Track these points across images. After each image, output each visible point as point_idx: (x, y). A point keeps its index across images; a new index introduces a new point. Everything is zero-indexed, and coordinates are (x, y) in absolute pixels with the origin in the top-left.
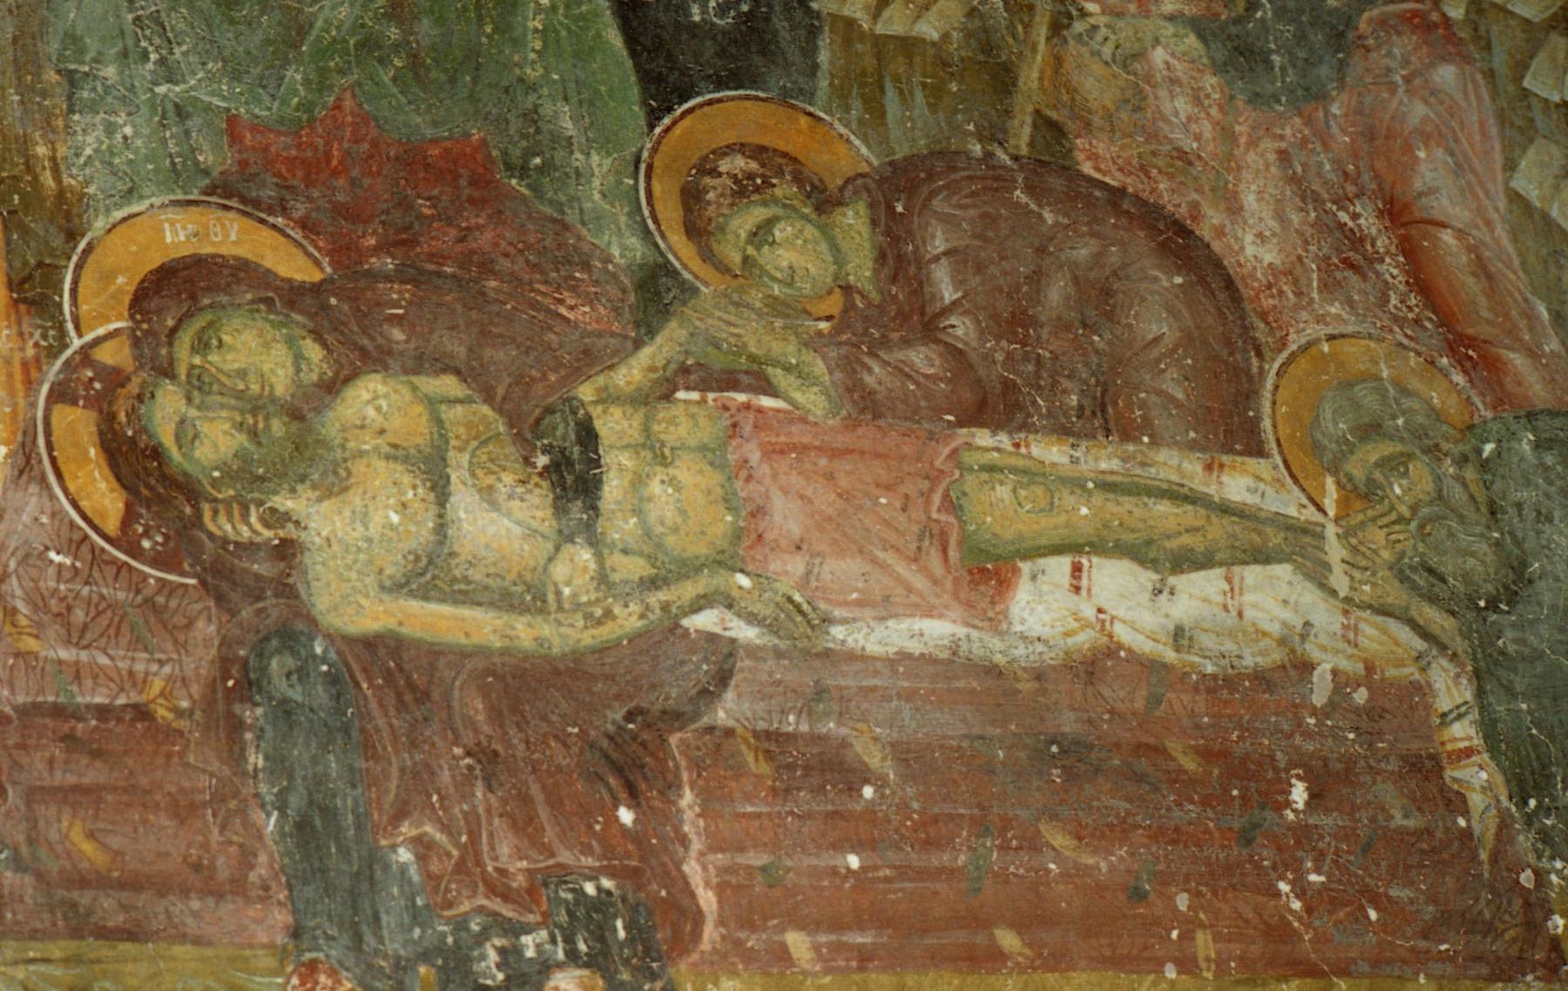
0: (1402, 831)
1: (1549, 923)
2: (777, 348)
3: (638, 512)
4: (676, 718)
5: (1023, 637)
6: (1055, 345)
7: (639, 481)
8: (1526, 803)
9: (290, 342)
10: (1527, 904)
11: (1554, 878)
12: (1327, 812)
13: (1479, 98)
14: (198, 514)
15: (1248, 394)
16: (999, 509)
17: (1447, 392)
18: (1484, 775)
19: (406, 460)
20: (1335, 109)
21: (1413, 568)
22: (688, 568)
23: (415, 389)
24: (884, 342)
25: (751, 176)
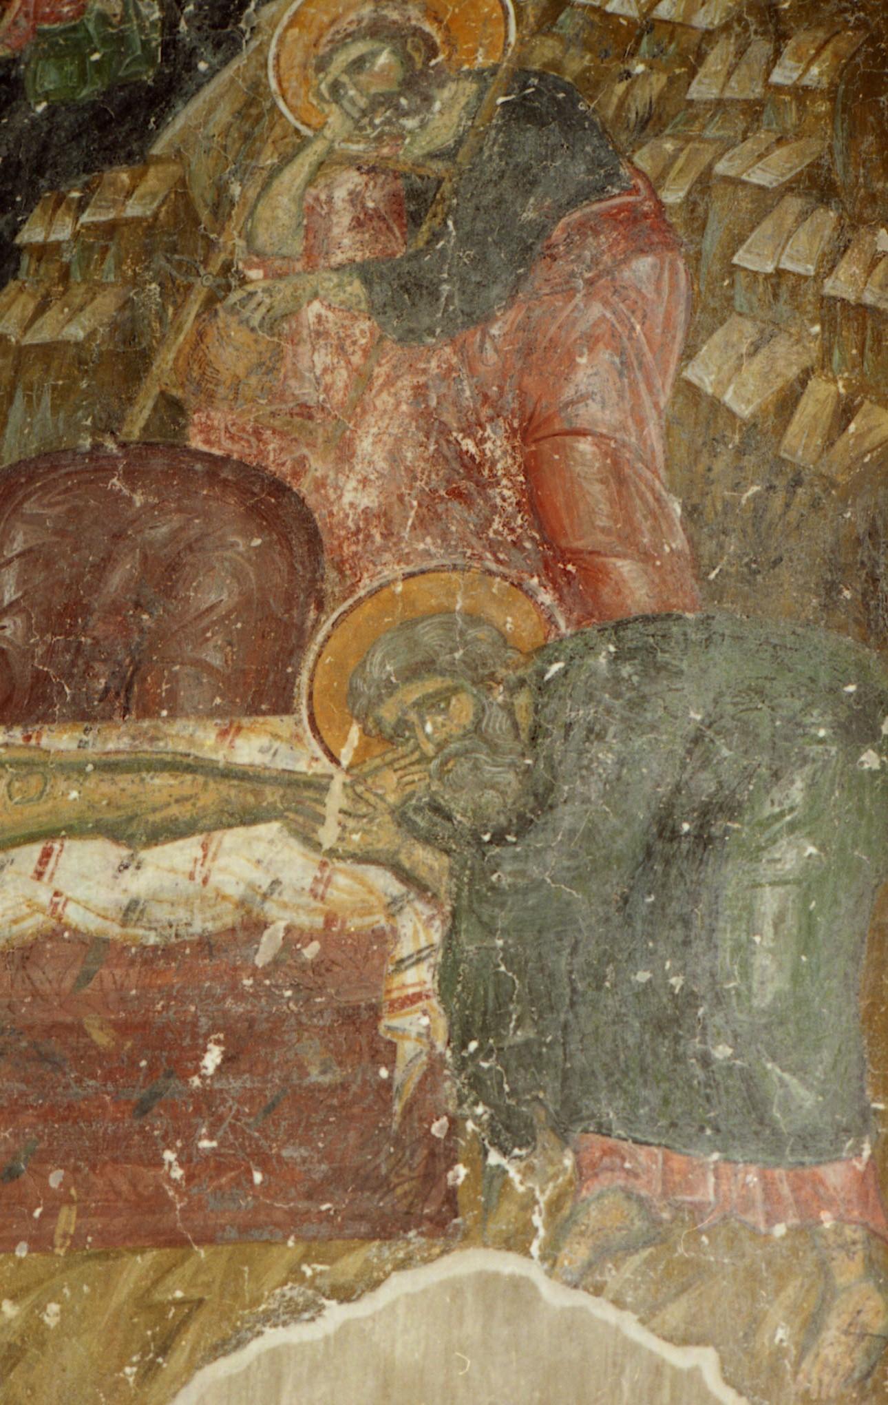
0: (319, 1088)
1: (450, 1175)
6: (100, 630)
8: (464, 1046)
10: (432, 1155)
11: (470, 1125)
12: (238, 1074)
13: (674, 286)
15: (294, 651)
17: (525, 612)
18: (425, 1021)
20: (495, 331)
21: (418, 810)
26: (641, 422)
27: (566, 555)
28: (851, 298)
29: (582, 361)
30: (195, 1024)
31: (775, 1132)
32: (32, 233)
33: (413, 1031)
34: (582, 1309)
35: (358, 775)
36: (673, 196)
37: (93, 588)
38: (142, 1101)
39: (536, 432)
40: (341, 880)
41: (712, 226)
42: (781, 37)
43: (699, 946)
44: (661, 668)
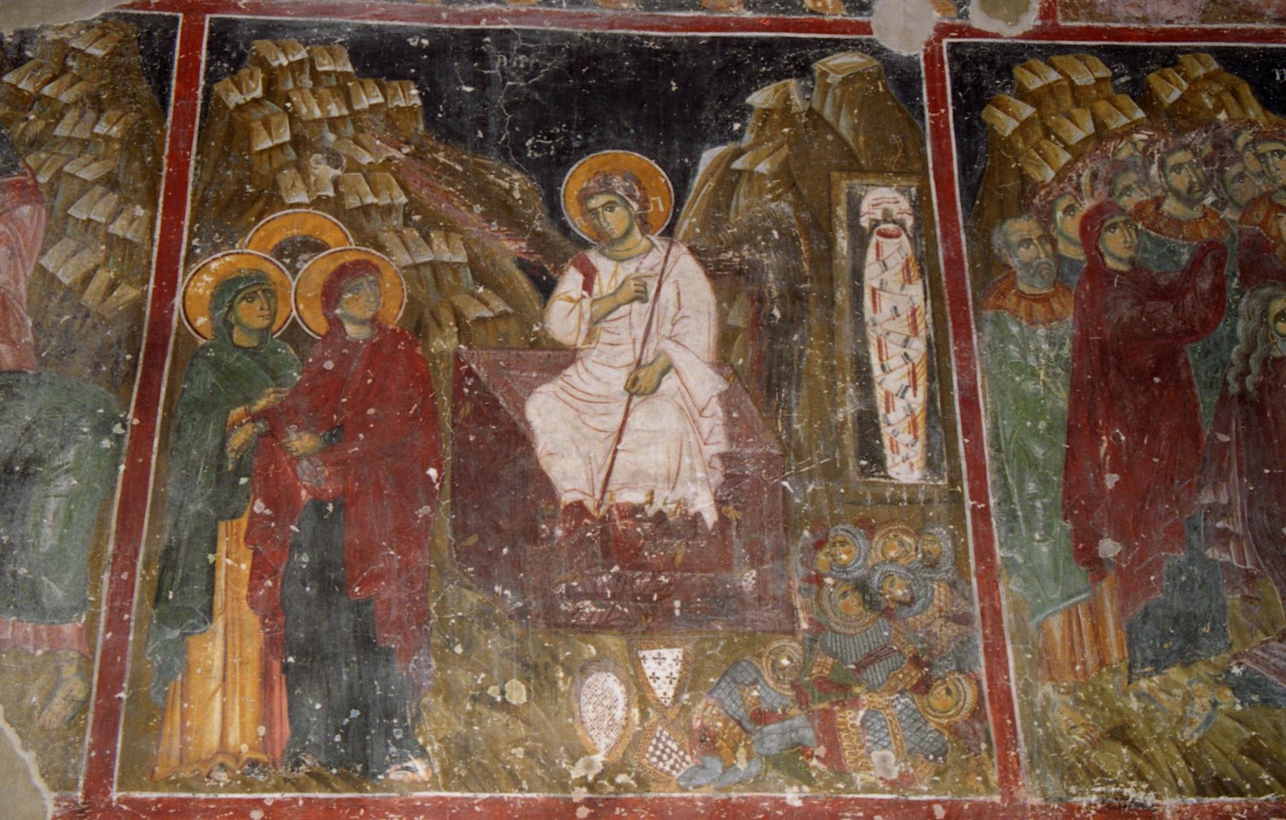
13: (39, 220)
26: (17, 282)
28: (120, 234)
31: (43, 608)
36: (43, 179)
42: (101, 111)
43: (16, 523)
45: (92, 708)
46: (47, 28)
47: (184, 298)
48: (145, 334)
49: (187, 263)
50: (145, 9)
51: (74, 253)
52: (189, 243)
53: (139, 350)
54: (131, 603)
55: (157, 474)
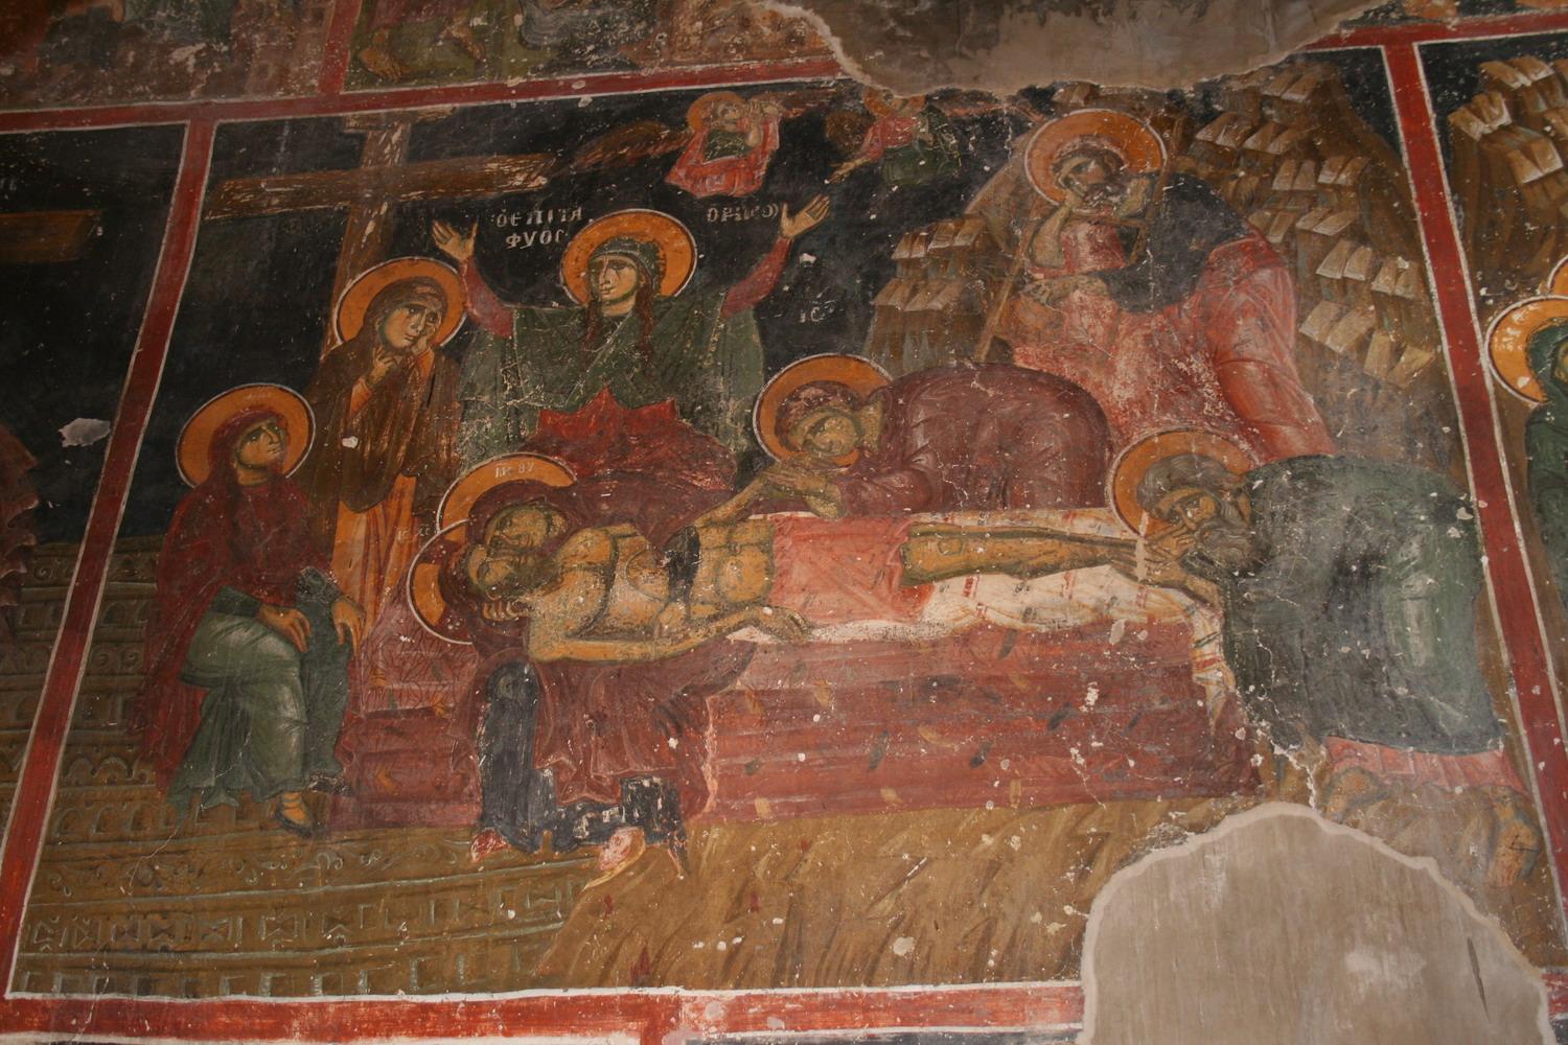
0: (1158, 713)
2: (813, 485)
3: (715, 581)
4: (712, 688)
5: (929, 624)
7: (718, 566)
8: (1247, 688)
9: (548, 518)
10: (1238, 749)
11: (1259, 732)
12: (1109, 704)
13: (1285, 285)
14: (481, 610)
16: (927, 556)
18: (1220, 674)
19: (595, 570)
20: (1185, 307)
21: (1192, 558)
22: (738, 607)
23: (607, 532)
24: (878, 474)
25: (817, 397)
26: (1281, 356)
27: (1250, 423)
28: (1388, 291)
29: (1240, 322)
30: (1078, 676)
31: (1444, 735)
32: (901, 253)
33: (1214, 680)
34: (1347, 837)
35: (1152, 540)
36: (1276, 238)
37: (974, 438)
38: (1052, 721)
39: (1223, 361)
40: (1153, 596)
41: (1301, 254)
43: (1375, 633)
44: (1320, 483)
45: (1551, 859)
46: (1230, 78)
47: (1491, 356)
48: (1457, 403)
49: (1482, 318)
50: (1336, 46)
51: (1339, 318)
52: (1476, 294)
53: (1457, 421)
54: (1557, 722)
55: (1532, 565)
